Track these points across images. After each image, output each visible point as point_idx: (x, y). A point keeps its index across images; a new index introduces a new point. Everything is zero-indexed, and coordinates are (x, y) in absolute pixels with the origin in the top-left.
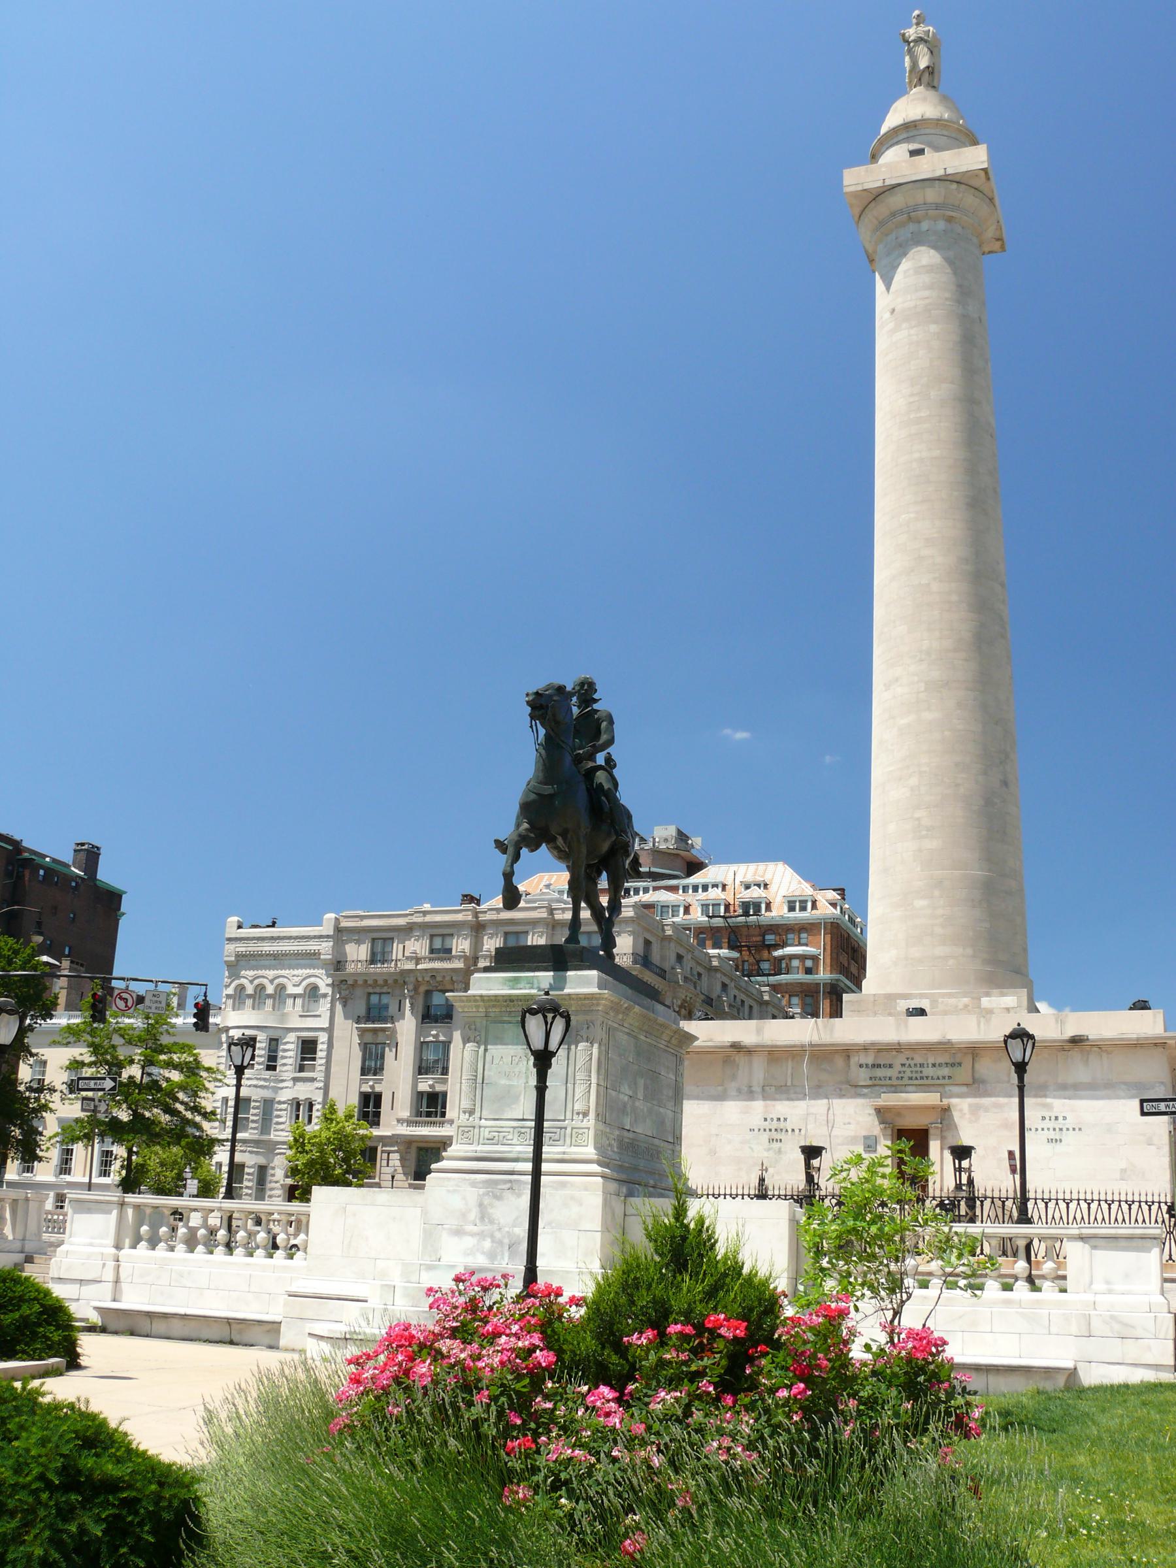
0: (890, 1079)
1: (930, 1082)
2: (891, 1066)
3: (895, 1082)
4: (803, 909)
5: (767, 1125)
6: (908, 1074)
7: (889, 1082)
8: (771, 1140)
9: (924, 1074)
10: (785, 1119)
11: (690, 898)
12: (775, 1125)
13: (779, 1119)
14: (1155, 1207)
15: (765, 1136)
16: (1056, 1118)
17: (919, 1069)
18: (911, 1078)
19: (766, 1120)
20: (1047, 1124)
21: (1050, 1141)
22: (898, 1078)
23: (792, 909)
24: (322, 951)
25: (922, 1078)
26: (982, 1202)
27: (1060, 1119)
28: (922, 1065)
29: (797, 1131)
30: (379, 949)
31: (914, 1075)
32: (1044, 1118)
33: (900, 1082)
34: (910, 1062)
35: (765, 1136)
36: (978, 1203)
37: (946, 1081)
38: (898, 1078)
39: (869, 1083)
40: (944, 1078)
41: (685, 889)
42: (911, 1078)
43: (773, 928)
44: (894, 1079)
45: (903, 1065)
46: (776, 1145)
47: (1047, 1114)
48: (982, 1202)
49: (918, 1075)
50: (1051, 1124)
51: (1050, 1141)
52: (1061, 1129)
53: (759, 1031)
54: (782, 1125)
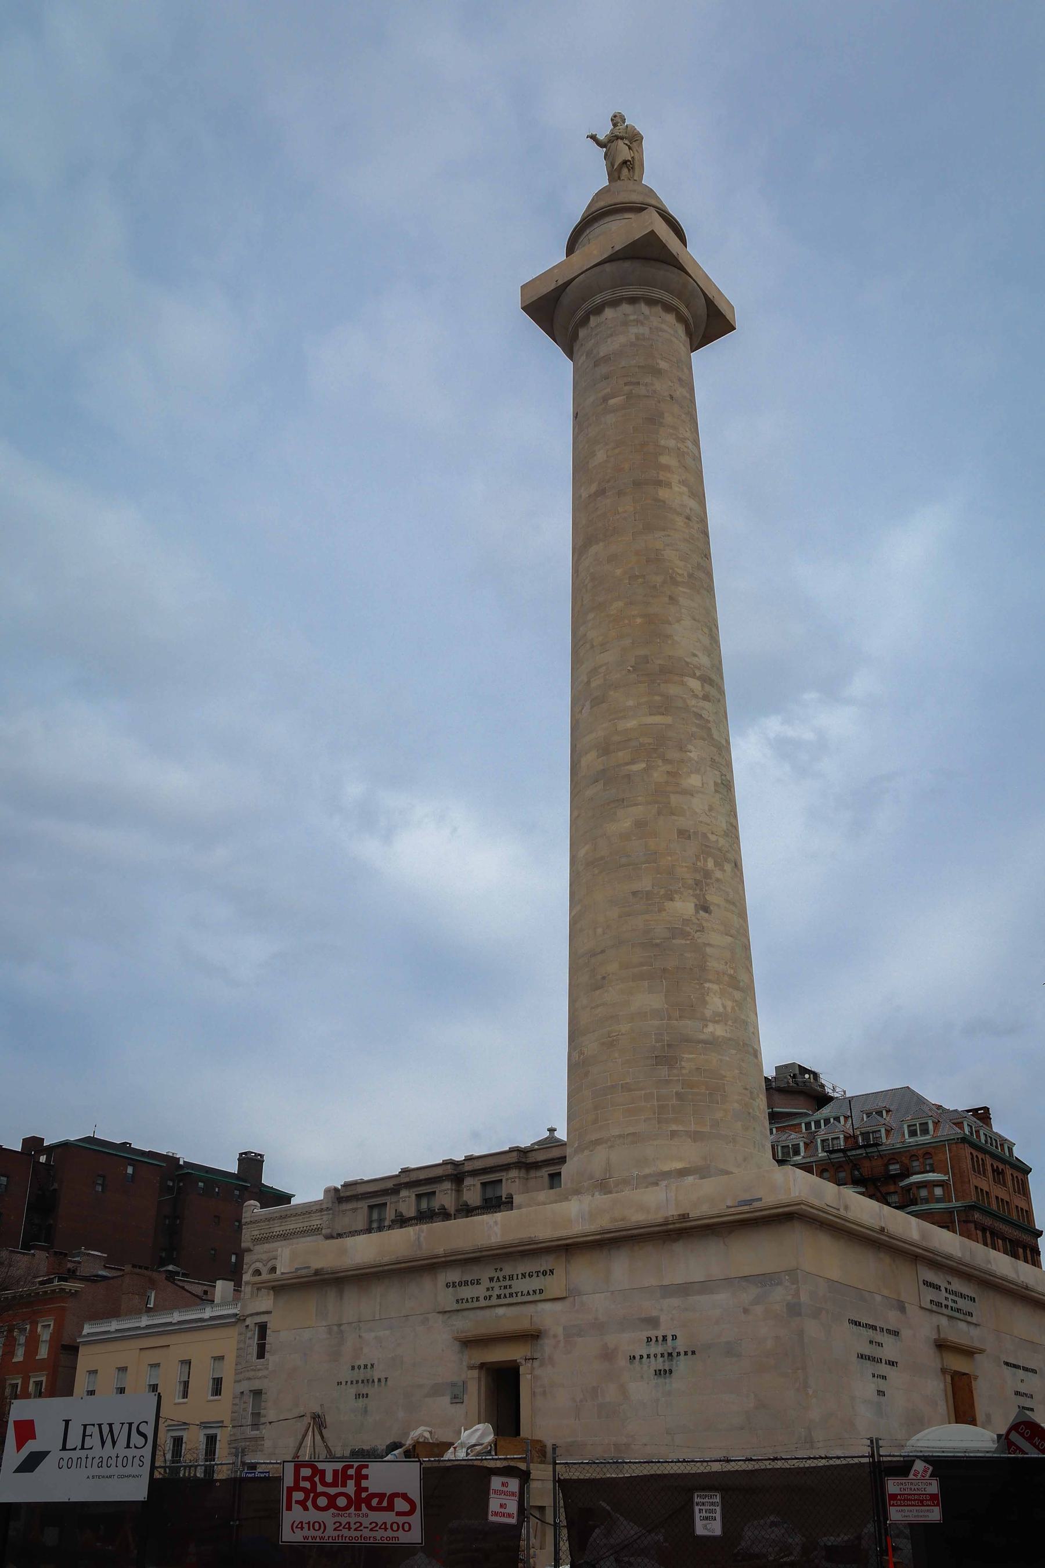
1: (520, 1299)
2: (478, 1283)
3: (483, 1303)
4: (925, 1131)
6: (497, 1291)
7: (476, 1304)
8: (358, 1396)
9: (513, 1291)
10: (372, 1365)
12: (361, 1375)
13: (366, 1366)
15: (352, 1391)
16: (664, 1338)
17: (507, 1283)
18: (499, 1297)
19: (353, 1368)
21: (658, 1373)
22: (485, 1298)
23: (913, 1133)
24: (324, 1226)
25: (511, 1295)
27: (669, 1338)
28: (511, 1278)
30: (375, 1216)
31: (502, 1292)
32: (649, 1340)
34: (500, 1274)
35: (352, 1391)
37: (537, 1297)
38: (485, 1298)
39: (456, 1307)
40: (534, 1292)
43: (894, 1156)
44: (481, 1299)
45: (491, 1279)
46: (361, 1402)
47: (652, 1333)
49: (507, 1291)
50: (658, 1349)
51: (658, 1373)
52: (670, 1355)
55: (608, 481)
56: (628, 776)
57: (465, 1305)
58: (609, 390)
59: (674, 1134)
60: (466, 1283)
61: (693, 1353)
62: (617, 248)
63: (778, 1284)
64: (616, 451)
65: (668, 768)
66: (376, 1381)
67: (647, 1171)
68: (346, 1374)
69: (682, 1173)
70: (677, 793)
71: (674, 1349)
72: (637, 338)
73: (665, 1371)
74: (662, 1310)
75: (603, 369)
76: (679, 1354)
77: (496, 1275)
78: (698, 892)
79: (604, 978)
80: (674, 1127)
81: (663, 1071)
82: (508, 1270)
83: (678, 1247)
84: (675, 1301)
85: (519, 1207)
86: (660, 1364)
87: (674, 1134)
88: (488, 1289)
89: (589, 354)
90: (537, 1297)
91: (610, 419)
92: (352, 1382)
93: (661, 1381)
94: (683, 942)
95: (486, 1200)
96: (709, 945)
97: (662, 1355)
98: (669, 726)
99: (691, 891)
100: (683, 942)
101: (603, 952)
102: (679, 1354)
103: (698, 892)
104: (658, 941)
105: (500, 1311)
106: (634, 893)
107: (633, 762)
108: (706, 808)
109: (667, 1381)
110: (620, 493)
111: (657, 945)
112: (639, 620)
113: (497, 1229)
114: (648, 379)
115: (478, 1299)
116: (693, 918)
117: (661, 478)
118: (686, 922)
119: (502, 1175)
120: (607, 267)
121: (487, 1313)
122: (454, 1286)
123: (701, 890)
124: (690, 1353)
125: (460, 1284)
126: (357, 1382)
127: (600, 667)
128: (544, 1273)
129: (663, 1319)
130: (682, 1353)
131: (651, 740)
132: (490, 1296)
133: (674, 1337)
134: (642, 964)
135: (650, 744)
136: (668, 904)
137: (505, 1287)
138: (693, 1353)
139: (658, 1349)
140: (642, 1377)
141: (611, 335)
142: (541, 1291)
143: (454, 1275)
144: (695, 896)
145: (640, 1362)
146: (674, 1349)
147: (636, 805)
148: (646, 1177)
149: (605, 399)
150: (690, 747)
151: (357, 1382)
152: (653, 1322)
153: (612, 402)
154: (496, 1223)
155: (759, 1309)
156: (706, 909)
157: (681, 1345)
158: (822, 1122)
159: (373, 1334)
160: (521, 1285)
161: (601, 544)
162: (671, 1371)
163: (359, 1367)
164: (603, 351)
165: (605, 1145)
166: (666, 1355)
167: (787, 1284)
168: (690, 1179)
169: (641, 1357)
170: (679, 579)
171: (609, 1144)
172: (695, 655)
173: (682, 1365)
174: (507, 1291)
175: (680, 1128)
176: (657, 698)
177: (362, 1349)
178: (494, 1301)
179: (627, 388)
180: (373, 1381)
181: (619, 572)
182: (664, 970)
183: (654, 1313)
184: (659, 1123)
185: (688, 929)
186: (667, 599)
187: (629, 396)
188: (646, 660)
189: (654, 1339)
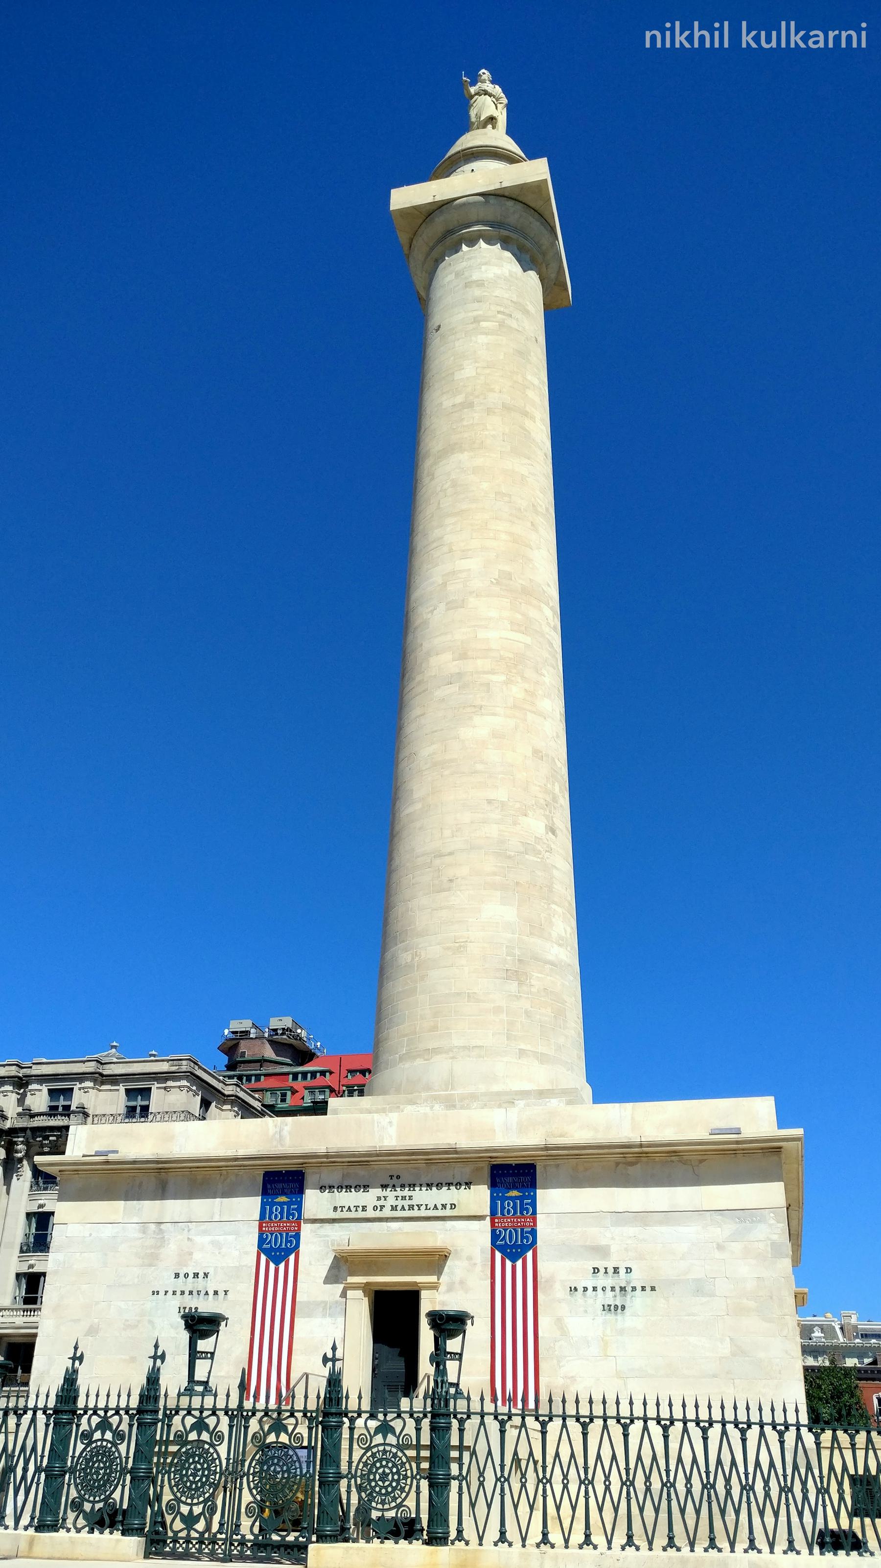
0: (364, 1208)
1: (423, 1213)
3: (370, 1213)
5: (180, 1284)
6: (391, 1201)
7: (361, 1214)
9: (414, 1202)
10: (206, 1275)
11: (299, 1084)
12: (190, 1284)
13: (196, 1275)
14: (790, 1437)
16: (616, 1270)
18: (394, 1208)
19: (177, 1276)
20: (602, 1281)
21: (607, 1308)
22: (375, 1208)
25: (411, 1207)
26: (461, 1422)
27: (622, 1271)
29: (221, 1294)
31: (400, 1203)
32: (596, 1270)
33: (378, 1214)
36: (455, 1423)
38: (375, 1208)
40: (444, 1206)
41: (295, 1076)
42: (394, 1208)
44: (370, 1209)
47: (601, 1265)
48: (461, 1422)
49: (406, 1203)
50: (609, 1281)
51: (607, 1308)
52: (623, 1289)
53: (169, 1138)
54: (200, 1284)
55: (478, 397)
56: (488, 685)
57: (346, 1215)
58: (480, 313)
59: (522, 1053)
61: (653, 1289)
62: (504, 185)
63: (760, 1221)
64: (488, 371)
65: (527, 686)
66: (211, 1293)
67: (496, 1088)
68: (168, 1282)
69: (542, 1094)
70: (534, 713)
71: (628, 1283)
72: (511, 275)
73: (616, 1307)
74: (613, 1238)
75: (477, 292)
76: (634, 1289)
78: (547, 813)
79: (451, 881)
80: (523, 1046)
81: (513, 986)
84: (632, 1230)
85: (335, 1112)
86: (609, 1298)
87: (522, 1053)
88: (379, 1199)
89: (457, 275)
90: (448, 1212)
91: (482, 339)
92: (174, 1293)
93: (610, 1317)
94: (535, 859)
95: (52, 1108)
96: (555, 867)
97: (613, 1289)
98: (527, 646)
99: (542, 811)
100: (535, 859)
101: (451, 854)
102: (634, 1289)
103: (547, 813)
104: (513, 854)
106: (489, 802)
107: (492, 672)
108: (555, 734)
109: (619, 1317)
110: (489, 411)
111: (509, 857)
112: (504, 536)
113: (393, 1131)
114: (518, 315)
115: (364, 1208)
116: (544, 837)
117: (527, 409)
118: (538, 839)
119: (77, 1086)
120: (492, 200)
123: (550, 812)
124: (648, 1289)
126: (183, 1293)
127: (461, 571)
129: (613, 1249)
130: (639, 1289)
131: (511, 656)
132: (382, 1207)
133: (629, 1270)
134: (495, 874)
135: (510, 659)
136: (522, 819)
137: (404, 1198)
138: (653, 1289)
139: (609, 1281)
140: (586, 1311)
141: (486, 264)
142: (453, 1206)
144: (547, 817)
145: (584, 1295)
146: (628, 1283)
147: (494, 714)
148: (498, 1094)
149: (476, 320)
150: (544, 672)
151: (183, 1293)
152: (602, 1251)
153: (484, 324)
155: (736, 1247)
156: (553, 832)
157: (637, 1278)
158: (309, 1075)
159: (207, 1239)
161: (466, 453)
162: (623, 1308)
163: (186, 1276)
164: (475, 276)
165: (444, 1055)
166: (618, 1289)
167: (772, 1222)
168: (554, 1103)
169: (585, 1289)
170: (539, 509)
171: (451, 1055)
172: (549, 585)
173: (637, 1302)
174: (406, 1203)
175: (528, 1047)
176: (519, 616)
177: (191, 1254)
178: (387, 1212)
179: (500, 316)
180: (207, 1293)
181: (485, 485)
182: (517, 883)
183: (603, 1242)
184: (508, 1039)
185: (539, 847)
186: (529, 524)
187: (502, 324)
188: (509, 576)
189: (602, 1271)
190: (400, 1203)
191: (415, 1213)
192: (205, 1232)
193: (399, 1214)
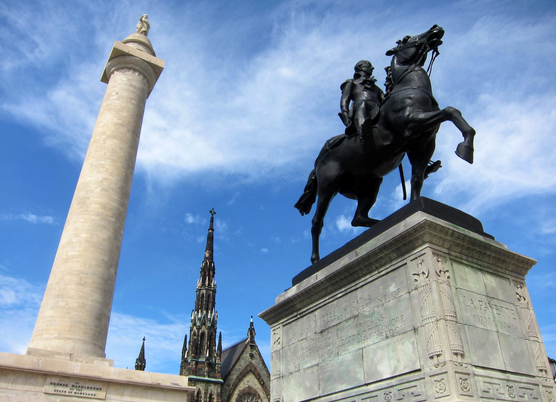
0: (65, 392)
1: (85, 396)
2: (67, 386)
3: (67, 393)
7: (64, 393)
18: (75, 393)
22: (69, 392)
25: (81, 393)
33: (69, 394)
34: (77, 384)
39: (53, 392)
40: (92, 395)
42: (75, 393)
44: (67, 392)
45: (73, 386)
57: (58, 393)
60: (61, 385)
77: (76, 385)
82: (81, 384)
83: (149, 392)
90: (93, 396)
105: (74, 399)
113: (78, 368)
115: (65, 392)
121: (68, 398)
122: (54, 384)
125: (58, 384)
128: (97, 389)
143: (56, 381)
154: (78, 366)
159: (5, 394)
160: (84, 391)
178: (73, 394)
190: (77, 392)
191: (82, 395)
192: (4, 392)
193: (77, 395)
